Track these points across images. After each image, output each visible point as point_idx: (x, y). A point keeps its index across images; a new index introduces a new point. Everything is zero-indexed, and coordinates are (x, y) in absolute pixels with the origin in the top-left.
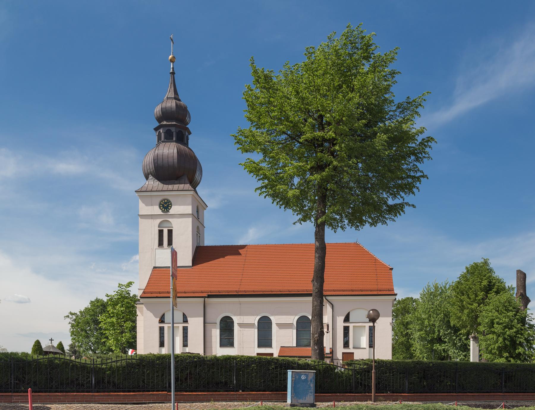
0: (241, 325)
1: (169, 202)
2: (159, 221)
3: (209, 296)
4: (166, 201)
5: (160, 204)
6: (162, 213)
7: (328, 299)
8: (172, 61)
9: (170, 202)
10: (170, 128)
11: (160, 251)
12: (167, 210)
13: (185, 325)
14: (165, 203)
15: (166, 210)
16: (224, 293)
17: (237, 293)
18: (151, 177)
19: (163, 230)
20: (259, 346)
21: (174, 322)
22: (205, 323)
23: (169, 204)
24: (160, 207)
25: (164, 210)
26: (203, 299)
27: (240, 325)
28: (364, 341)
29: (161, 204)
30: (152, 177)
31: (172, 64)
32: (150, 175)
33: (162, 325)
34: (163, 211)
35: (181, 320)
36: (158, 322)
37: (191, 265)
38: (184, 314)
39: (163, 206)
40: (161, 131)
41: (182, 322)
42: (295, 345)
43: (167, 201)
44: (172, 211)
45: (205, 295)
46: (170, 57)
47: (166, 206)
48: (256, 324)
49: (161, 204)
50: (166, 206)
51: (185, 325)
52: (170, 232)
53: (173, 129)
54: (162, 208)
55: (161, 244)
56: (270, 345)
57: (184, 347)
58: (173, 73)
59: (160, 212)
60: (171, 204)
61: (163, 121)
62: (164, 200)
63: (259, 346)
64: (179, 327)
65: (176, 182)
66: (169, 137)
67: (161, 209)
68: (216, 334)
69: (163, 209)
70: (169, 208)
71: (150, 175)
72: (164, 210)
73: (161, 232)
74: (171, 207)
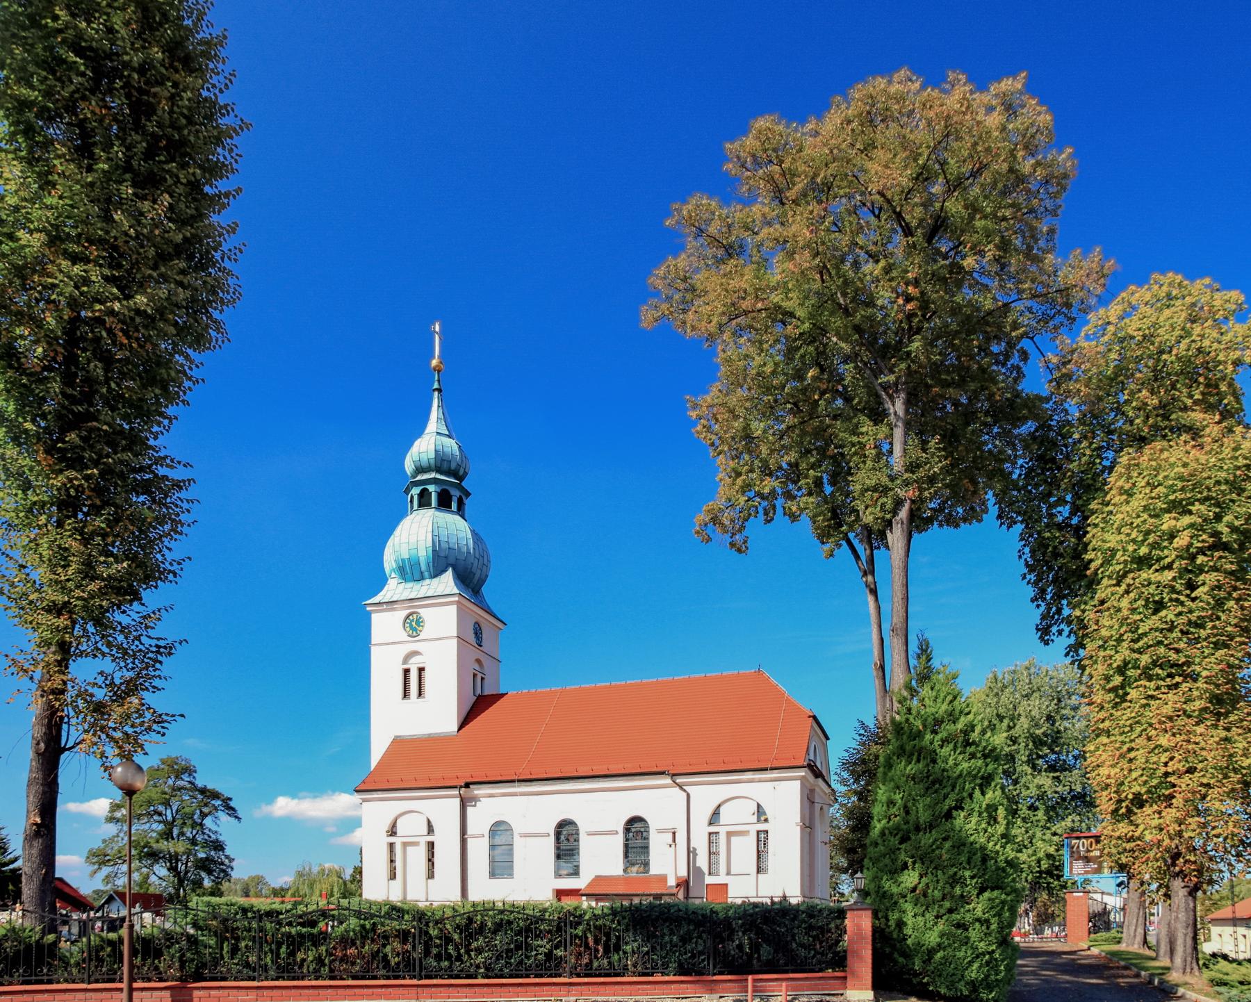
10: (428, 487)
33: (392, 839)
51: (430, 838)
53: (431, 488)
55: (406, 694)
59: (404, 636)
73: (407, 671)
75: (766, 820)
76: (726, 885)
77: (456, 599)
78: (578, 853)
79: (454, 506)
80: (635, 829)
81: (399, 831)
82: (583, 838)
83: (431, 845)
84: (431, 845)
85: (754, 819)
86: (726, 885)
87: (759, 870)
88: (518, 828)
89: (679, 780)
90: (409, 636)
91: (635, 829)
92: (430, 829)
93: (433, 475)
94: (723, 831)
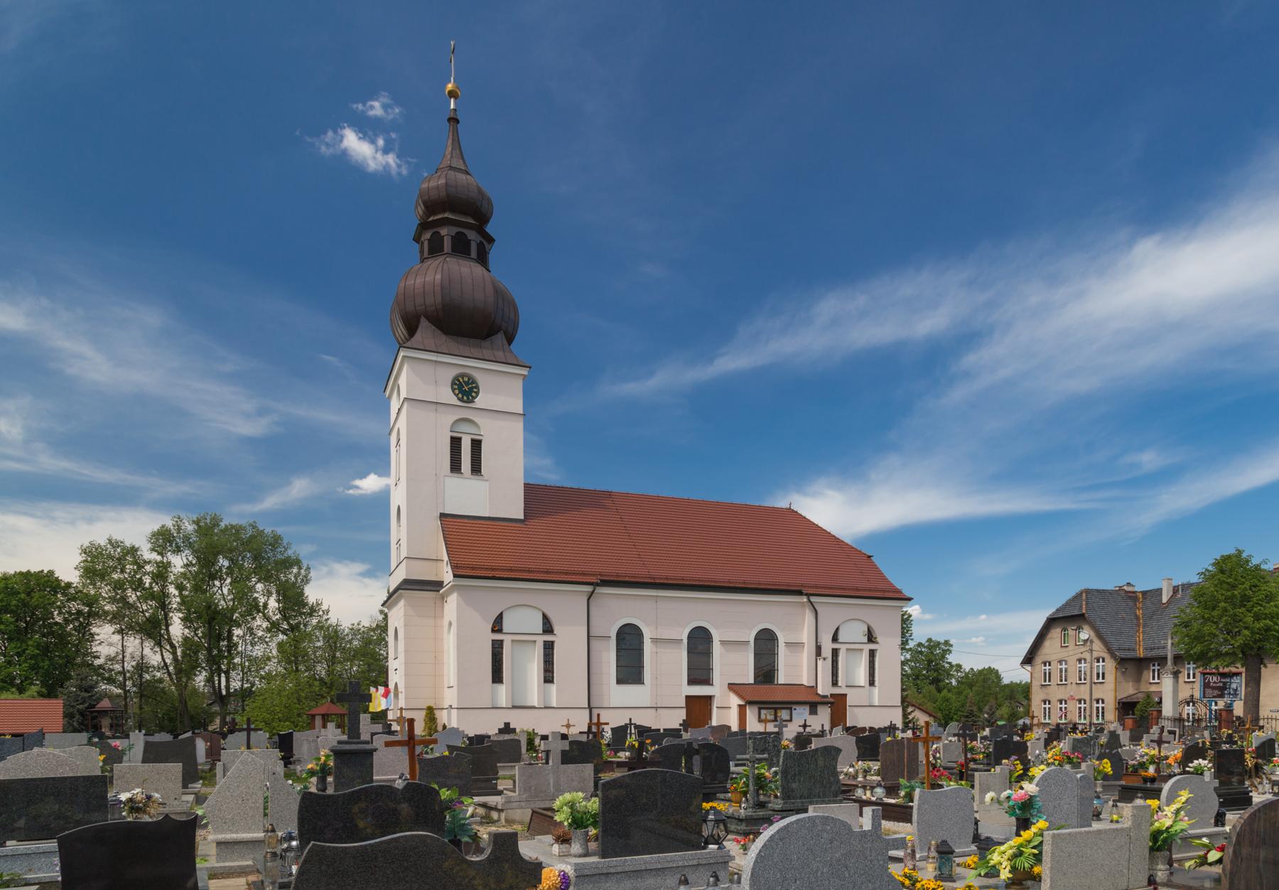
0: (655, 641)
1: (473, 383)
2: (451, 417)
4: (466, 379)
5: (453, 383)
6: (460, 403)
8: (452, 94)
9: (474, 382)
11: (453, 482)
12: (468, 398)
13: (549, 638)
14: (467, 383)
15: (465, 398)
16: (627, 579)
17: (652, 581)
18: (424, 323)
19: (460, 439)
20: (692, 681)
22: (589, 636)
23: (473, 388)
24: (453, 390)
25: (463, 397)
26: (589, 589)
27: (655, 641)
28: (861, 677)
29: (456, 384)
30: (427, 322)
31: (452, 100)
32: (423, 320)
33: (498, 637)
34: (461, 400)
35: (539, 628)
37: (522, 517)
38: (545, 617)
39: (460, 386)
40: (444, 231)
41: (541, 632)
42: (752, 681)
43: (469, 379)
44: (480, 401)
45: (594, 580)
46: (450, 86)
47: (466, 389)
48: (685, 641)
49: (456, 384)
50: (466, 389)
51: (549, 638)
52: (476, 445)
53: (472, 235)
54: (457, 392)
55: (455, 466)
56: (707, 681)
57: (495, 685)
58: (454, 120)
59: (454, 401)
60: (477, 387)
61: (444, 211)
62: (463, 375)
63: (692, 681)
64: (535, 641)
65: (487, 343)
66: (461, 247)
67: (457, 395)
68: (608, 658)
69: (460, 396)
70: (474, 394)
71: (423, 319)
72: (463, 397)
73: (456, 443)
74: (477, 393)
75: (874, 642)
76: (846, 695)
78: (904, 676)
79: (474, 254)
80: (766, 643)
83: (549, 647)
84: (549, 647)
85: (865, 640)
86: (846, 695)
87: (872, 683)
88: (716, 637)
89: (813, 599)
90: (459, 399)
91: (766, 643)
92: (548, 628)
93: (471, 221)
94: (843, 648)
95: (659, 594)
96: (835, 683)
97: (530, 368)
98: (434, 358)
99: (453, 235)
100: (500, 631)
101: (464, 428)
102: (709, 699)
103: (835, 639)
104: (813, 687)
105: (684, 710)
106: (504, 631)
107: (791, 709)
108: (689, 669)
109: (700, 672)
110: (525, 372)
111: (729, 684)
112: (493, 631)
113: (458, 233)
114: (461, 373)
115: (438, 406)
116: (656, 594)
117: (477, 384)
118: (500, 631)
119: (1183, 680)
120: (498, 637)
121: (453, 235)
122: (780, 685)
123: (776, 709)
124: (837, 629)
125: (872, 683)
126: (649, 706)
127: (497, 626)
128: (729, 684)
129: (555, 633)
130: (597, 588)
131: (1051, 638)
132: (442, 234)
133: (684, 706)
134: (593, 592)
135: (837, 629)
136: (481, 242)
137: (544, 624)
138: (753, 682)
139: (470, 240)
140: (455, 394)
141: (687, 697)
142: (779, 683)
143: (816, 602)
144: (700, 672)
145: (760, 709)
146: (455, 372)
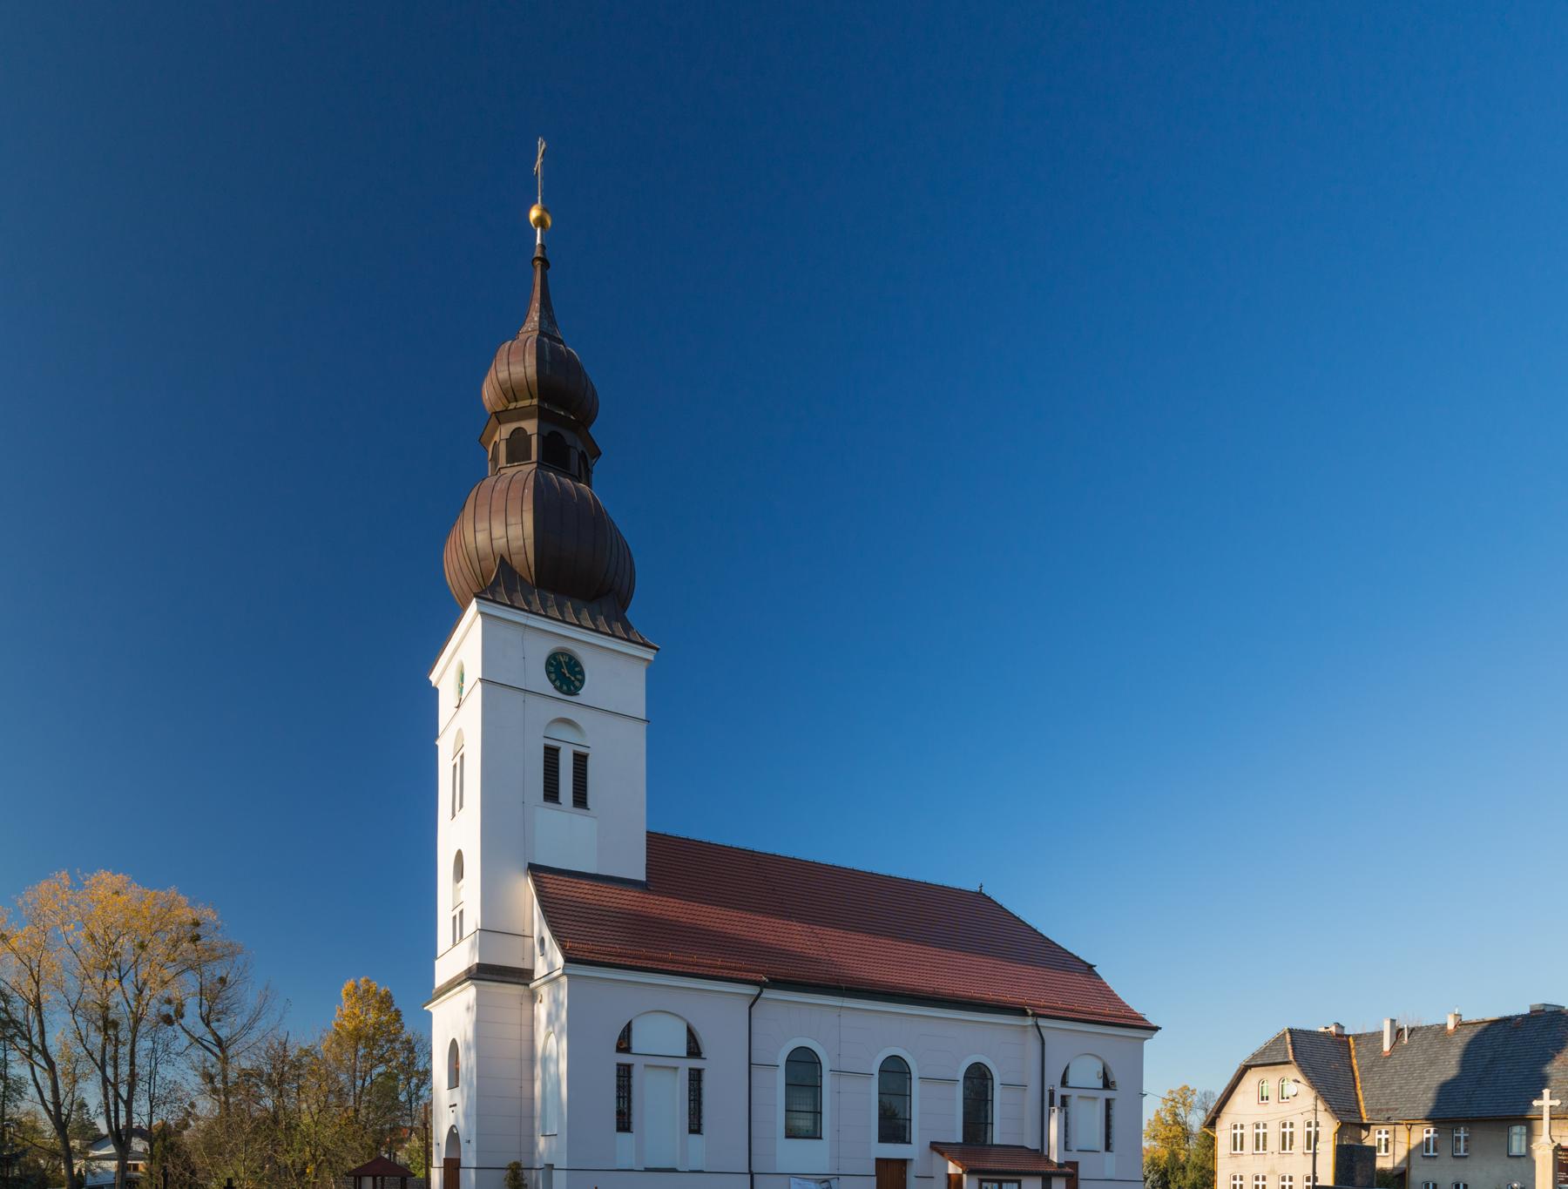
3: (778, 983)
5: (548, 663)
7: (1040, 1024)
12: (569, 688)
13: (695, 1063)
15: (565, 688)
20: (884, 1138)
21: (753, 1062)
22: (750, 1064)
26: (753, 990)
29: (552, 665)
33: (625, 1058)
34: (559, 689)
36: (615, 1049)
38: (691, 1033)
44: (585, 695)
48: (877, 1075)
49: (552, 665)
52: (580, 761)
54: (553, 676)
55: (551, 794)
59: (549, 688)
63: (884, 1138)
67: (553, 682)
69: (558, 683)
73: (551, 755)
77: (651, 657)
80: (978, 1082)
81: (637, 1045)
82: (916, 1087)
83: (696, 1077)
84: (696, 1077)
85: (1100, 1084)
87: (1108, 1148)
89: (1042, 1022)
90: (556, 688)
91: (978, 1082)
92: (694, 1050)
95: (845, 1004)
96: (1067, 1148)
97: (657, 649)
98: (523, 621)
99: (546, 435)
100: (627, 1050)
101: (565, 734)
102: (903, 1163)
103: (1064, 1083)
104: (1037, 1150)
105: (875, 1178)
106: (634, 1051)
107: (1019, 1182)
108: (880, 1118)
109: (893, 1126)
110: (650, 655)
111: (931, 1142)
112: (619, 1050)
113: (552, 434)
114: (561, 648)
115: (527, 695)
116: (840, 1004)
117: (581, 666)
118: (627, 1050)
119: (1420, 1154)
120: (625, 1058)
121: (546, 435)
122: (996, 1146)
123: (1000, 1182)
124: (1067, 1068)
125: (1108, 1148)
126: (828, 1173)
127: (624, 1045)
128: (931, 1142)
129: (703, 1056)
130: (765, 990)
131: (1244, 1092)
132: (529, 433)
133: (874, 1174)
134: (758, 996)
135: (1067, 1068)
136: (582, 451)
137: (689, 1043)
138: (961, 1140)
139: (570, 446)
140: (550, 679)
141: (878, 1160)
142: (994, 1143)
143: (1043, 1027)
144: (893, 1126)
145: (981, 1181)
146: (547, 647)
